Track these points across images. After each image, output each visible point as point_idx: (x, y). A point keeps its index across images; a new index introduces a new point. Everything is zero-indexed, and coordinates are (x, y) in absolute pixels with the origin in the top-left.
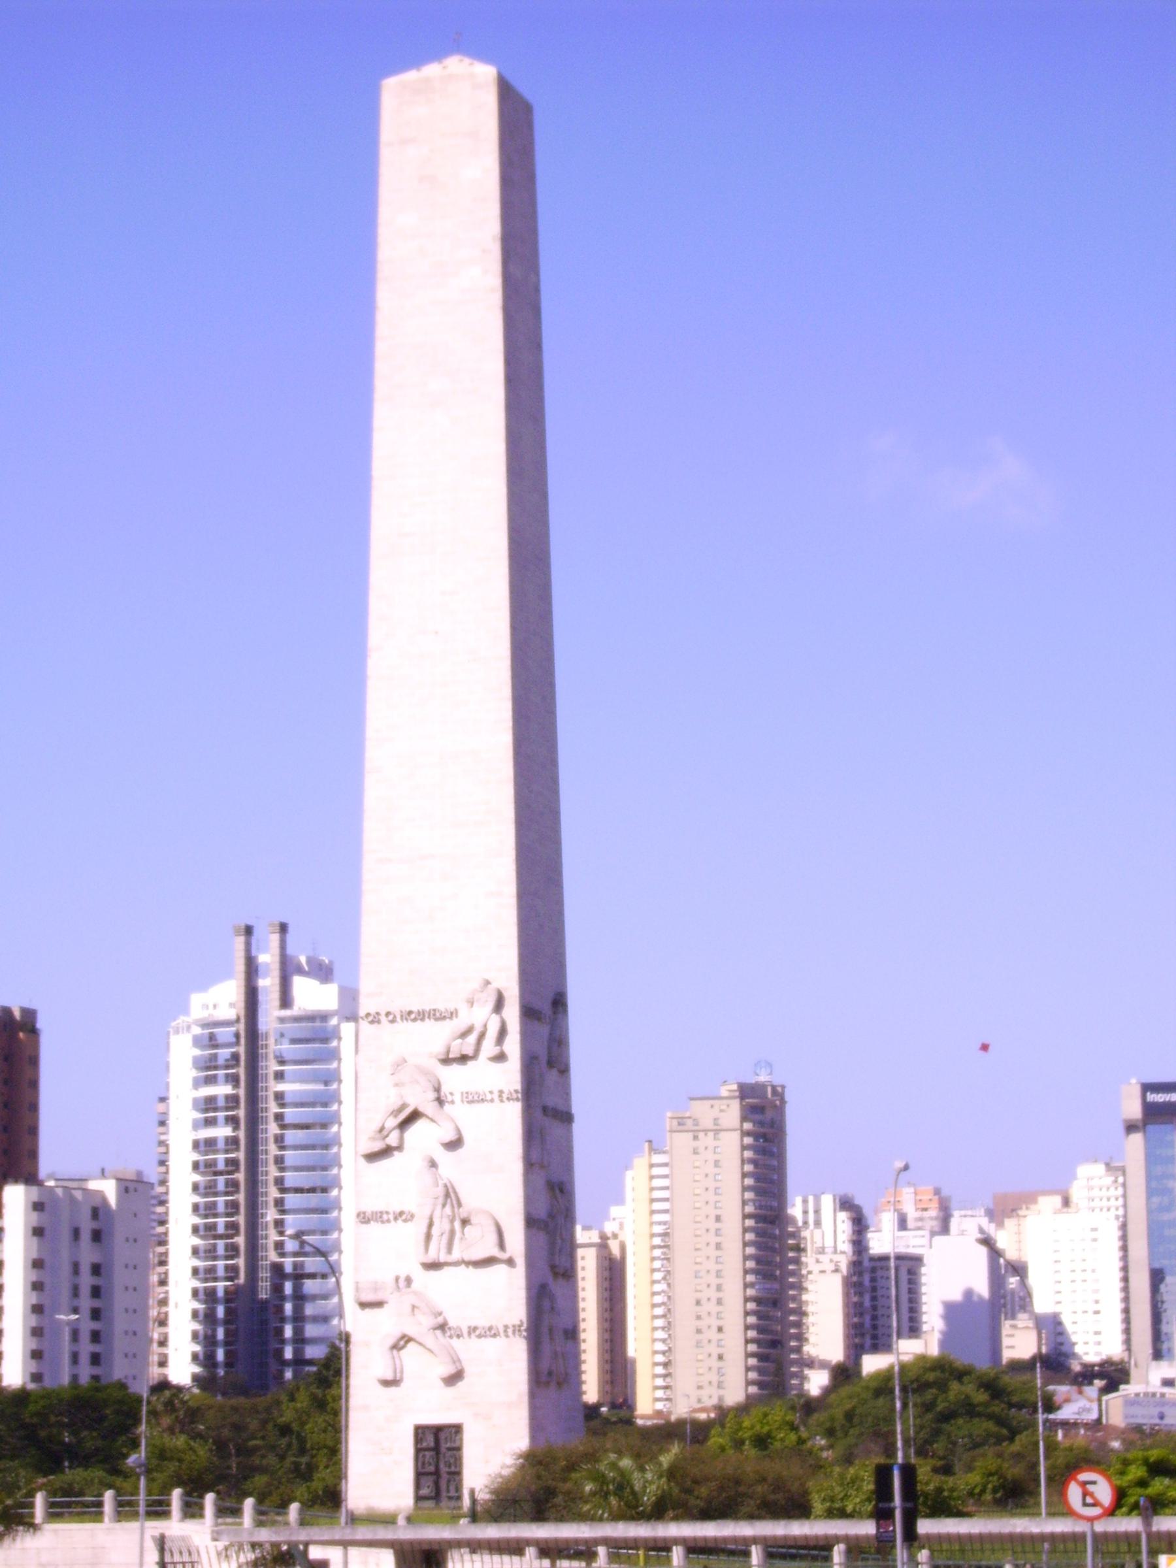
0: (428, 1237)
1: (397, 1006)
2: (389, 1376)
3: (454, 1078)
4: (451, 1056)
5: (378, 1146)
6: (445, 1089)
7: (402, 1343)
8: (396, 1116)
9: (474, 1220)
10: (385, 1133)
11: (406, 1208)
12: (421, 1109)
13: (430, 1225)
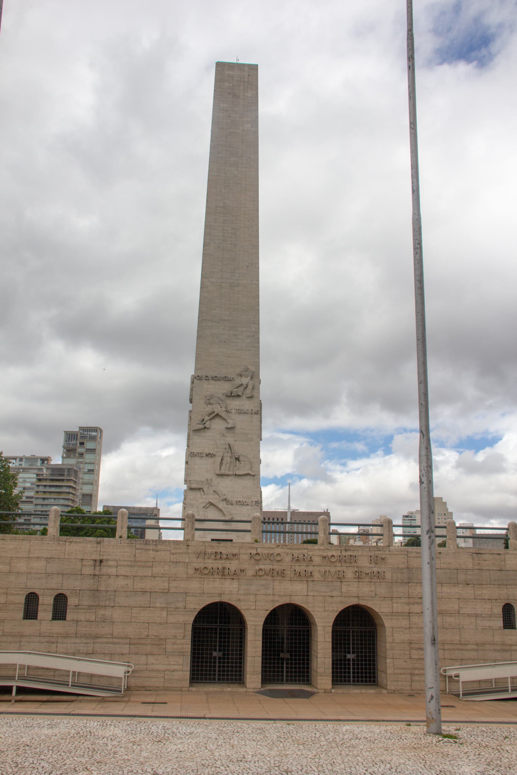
0: (221, 464)
1: (211, 374)
3: (234, 404)
4: (233, 395)
5: (202, 426)
6: (229, 408)
7: (208, 505)
8: (209, 416)
9: (241, 459)
10: (204, 422)
11: (211, 453)
12: (220, 414)
13: (222, 460)
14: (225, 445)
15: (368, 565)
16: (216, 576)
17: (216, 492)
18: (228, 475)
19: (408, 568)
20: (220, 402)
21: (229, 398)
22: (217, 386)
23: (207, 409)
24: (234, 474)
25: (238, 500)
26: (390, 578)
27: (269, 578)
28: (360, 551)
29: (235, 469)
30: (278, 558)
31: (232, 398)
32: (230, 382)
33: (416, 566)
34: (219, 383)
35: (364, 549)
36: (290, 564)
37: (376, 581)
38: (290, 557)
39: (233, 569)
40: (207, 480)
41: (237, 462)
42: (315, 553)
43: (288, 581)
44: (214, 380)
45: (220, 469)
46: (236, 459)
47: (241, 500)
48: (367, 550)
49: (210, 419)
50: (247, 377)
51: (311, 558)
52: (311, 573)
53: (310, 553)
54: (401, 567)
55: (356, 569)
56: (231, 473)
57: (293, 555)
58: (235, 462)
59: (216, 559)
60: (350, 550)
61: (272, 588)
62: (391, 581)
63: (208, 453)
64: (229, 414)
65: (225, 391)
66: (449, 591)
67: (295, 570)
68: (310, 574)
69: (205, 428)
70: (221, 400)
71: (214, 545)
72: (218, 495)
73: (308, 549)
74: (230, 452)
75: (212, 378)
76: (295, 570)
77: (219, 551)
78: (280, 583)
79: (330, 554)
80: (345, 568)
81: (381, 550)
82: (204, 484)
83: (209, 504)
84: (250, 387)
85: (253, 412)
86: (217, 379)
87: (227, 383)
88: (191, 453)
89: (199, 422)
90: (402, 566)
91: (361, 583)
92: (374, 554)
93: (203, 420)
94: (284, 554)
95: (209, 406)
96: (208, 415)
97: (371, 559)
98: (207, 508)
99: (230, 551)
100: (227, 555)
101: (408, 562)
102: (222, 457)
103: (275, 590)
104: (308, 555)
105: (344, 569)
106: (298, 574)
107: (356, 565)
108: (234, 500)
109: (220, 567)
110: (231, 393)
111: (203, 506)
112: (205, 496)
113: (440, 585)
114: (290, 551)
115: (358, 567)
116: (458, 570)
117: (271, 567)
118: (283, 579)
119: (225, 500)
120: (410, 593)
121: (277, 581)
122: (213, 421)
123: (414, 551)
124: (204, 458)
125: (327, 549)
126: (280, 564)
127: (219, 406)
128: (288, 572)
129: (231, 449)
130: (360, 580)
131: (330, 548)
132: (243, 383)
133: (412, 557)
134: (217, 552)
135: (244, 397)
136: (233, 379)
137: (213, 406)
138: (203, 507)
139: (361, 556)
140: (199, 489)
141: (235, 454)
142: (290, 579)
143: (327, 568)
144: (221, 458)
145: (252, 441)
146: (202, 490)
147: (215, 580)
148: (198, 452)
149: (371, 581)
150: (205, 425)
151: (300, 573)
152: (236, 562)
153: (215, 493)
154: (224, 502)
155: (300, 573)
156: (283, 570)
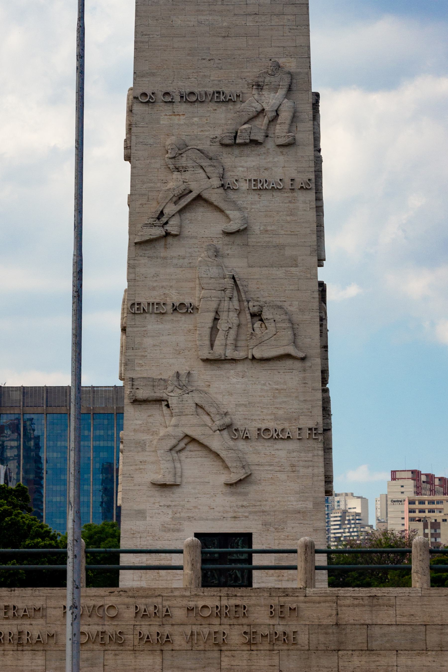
0: (214, 330)
2: (169, 480)
4: (238, 141)
5: (158, 232)
6: (230, 178)
8: (176, 203)
10: (164, 220)
11: (187, 301)
12: (206, 195)
13: (216, 319)
14: (222, 281)
15: (268, 621)
16: (8, 647)
17: (201, 407)
18: (233, 360)
19: (337, 624)
20: (205, 163)
21: (229, 149)
22: (196, 119)
23: (171, 185)
24: (250, 357)
25: (263, 426)
26: (307, 642)
27: (96, 647)
28: (254, 598)
29: (252, 343)
30: (113, 613)
31: (237, 151)
32: (230, 106)
33: (352, 622)
34: (200, 109)
35: (261, 594)
36: (133, 623)
37: (280, 648)
38: (133, 610)
39: (35, 634)
40: (178, 375)
41: (257, 324)
42: (175, 602)
43: (129, 652)
44: (187, 101)
45: (212, 346)
46: (253, 315)
47: (271, 425)
48: (266, 594)
49: (180, 212)
50: (276, 90)
51: (167, 611)
52: (168, 637)
53: (166, 603)
54: (324, 623)
55: (246, 629)
56: (241, 354)
57: (136, 607)
58: (250, 325)
59: (7, 618)
60: (236, 596)
61: (102, 665)
62: (307, 647)
63: (177, 304)
64: (231, 194)
65: (218, 132)
66: (409, 663)
67: (140, 633)
68: (165, 639)
69: (168, 234)
70: (207, 157)
71: (3, 595)
72: (208, 414)
73: (162, 596)
74: (235, 299)
75: (182, 97)
76: (140, 633)
77: (11, 604)
78: (116, 655)
79: (201, 603)
80: (228, 627)
81: (291, 594)
82: (170, 388)
83: (186, 441)
84: (285, 116)
85: (297, 185)
86: (194, 98)
87: (223, 108)
88: (133, 304)
89: (151, 221)
90: (326, 622)
91: (255, 652)
92: (277, 602)
93: (162, 213)
94: (123, 606)
95: (176, 175)
96: (174, 199)
97: (272, 610)
98: (180, 451)
99: (30, 604)
100: (25, 611)
101: (337, 614)
102: (217, 312)
103: (106, 667)
104: (163, 607)
105: (225, 628)
106: (145, 640)
107: (245, 621)
108: (253, 427)
109: (15, 631)
110: (235, 137)
111: (169, 447)
112: (174, 421)
113: (395, 652)
114: (131, 600)
115: (249, 625)
116: (428, 627)
117: (100, 628)
118: (121, 648)
119: (228, 427)
120: (340, 668)
121: (111, 652)
122: (188, 215)
123: (349, 595)
124: (167, 318)
125: (196, 595)
126: (116, 623)
127: (203, 175)
128: (128, 636)
129: (238, 291)
130: (253, 648)
131: (202, 594)
132: (267, 108)
133: (345, 606)
134: (8, 606)
135: (270, 144)
136: (238, 96)
137: (187, 176)
138: (171, 450)
139: (255, 605)
140: (159, 401)
141: (251, 304)
142: (132, 648)
143: (195, 629)
144: (212, 315)
145: (296, 266)
146: (164, 403)
147: (6, 653)
148: (151, 301)
149: (271, 648)
150: (168, 228)
151: (148, 638)
152: (41, 621)
153: (200, 410)
154: (225, 433)
155: (148, 638)
156: (120, 633)
